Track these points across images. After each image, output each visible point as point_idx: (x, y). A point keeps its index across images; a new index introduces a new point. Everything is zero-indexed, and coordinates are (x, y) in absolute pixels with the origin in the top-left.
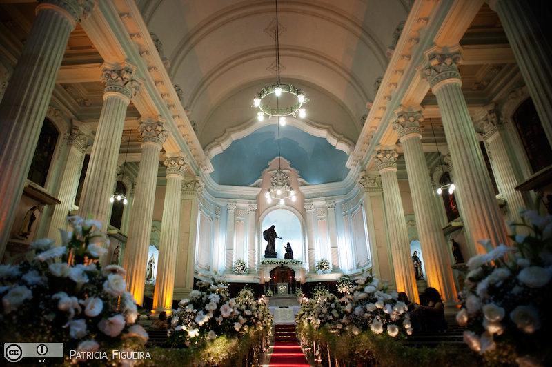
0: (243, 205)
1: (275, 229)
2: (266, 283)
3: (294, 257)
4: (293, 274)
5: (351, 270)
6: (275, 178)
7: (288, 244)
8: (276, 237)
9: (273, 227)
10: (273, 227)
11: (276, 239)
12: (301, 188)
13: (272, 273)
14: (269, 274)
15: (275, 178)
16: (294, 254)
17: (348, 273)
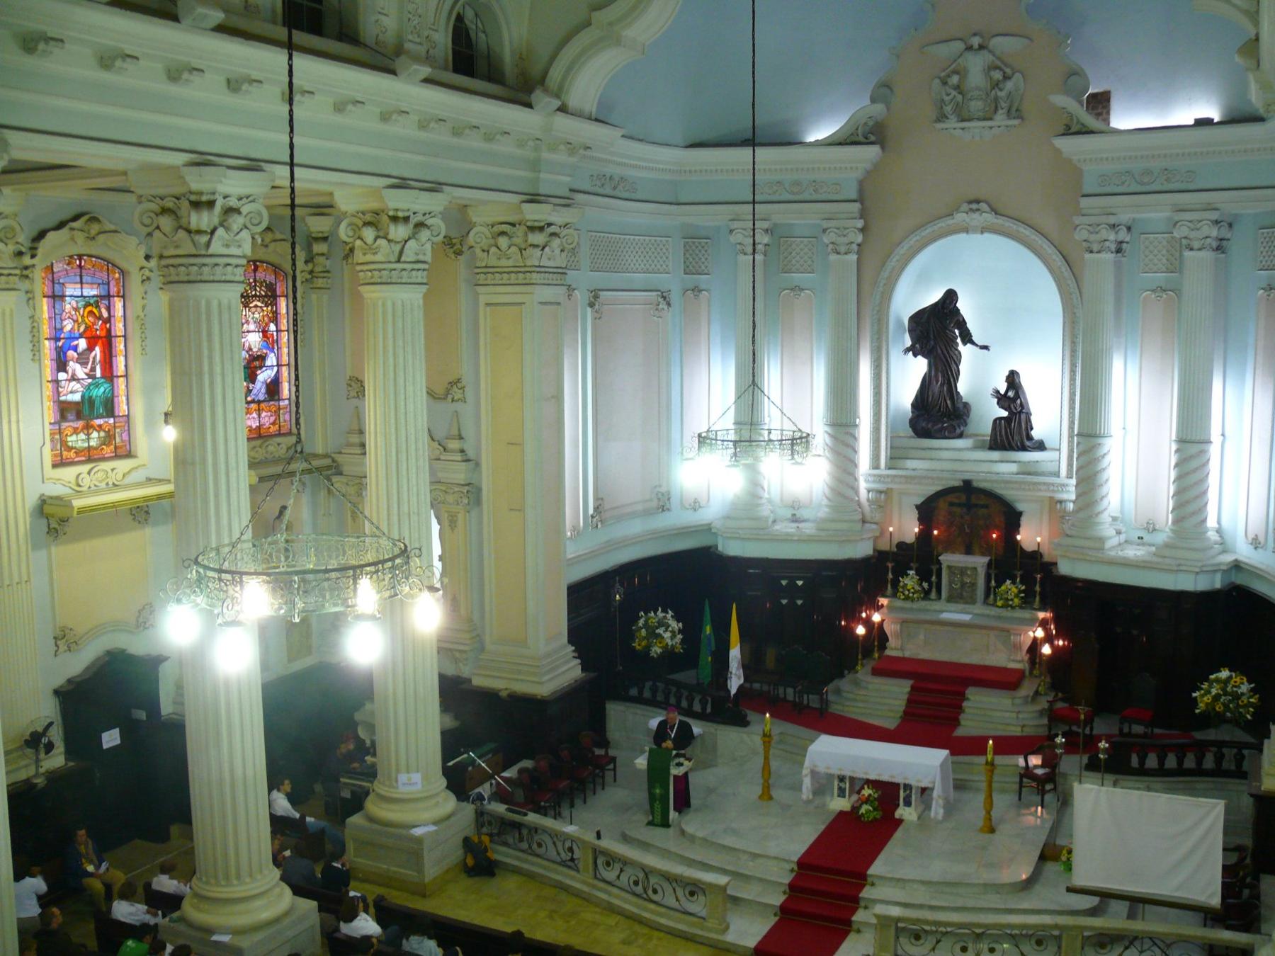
0: (801, 218)
1: (963, 305)
2: (901, 545)
3: (1036, 434)
4: (1012, 519)
5: (1256, 543)
6: (955, 79)
7: (1013, 379)
8: (967, 338)
9: (951, 296)
10: (951, 296)
11: (965, 350)
12: (1068, 145)
13: (926, 511)
14: (915, 514)
15: (955, 79)
16: (1034, 420)
17: (1244, 552)
